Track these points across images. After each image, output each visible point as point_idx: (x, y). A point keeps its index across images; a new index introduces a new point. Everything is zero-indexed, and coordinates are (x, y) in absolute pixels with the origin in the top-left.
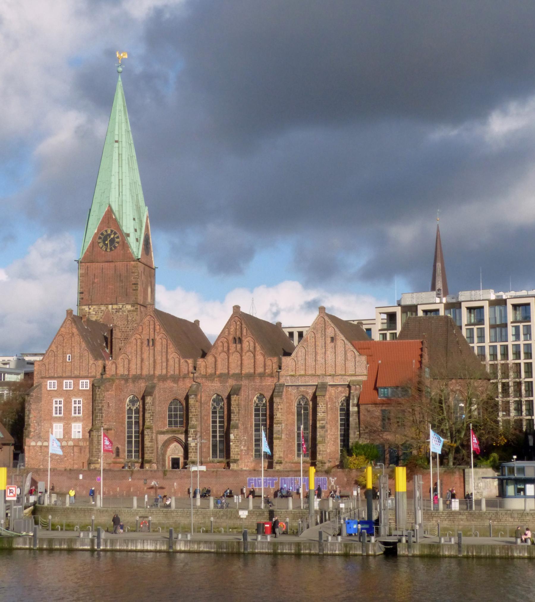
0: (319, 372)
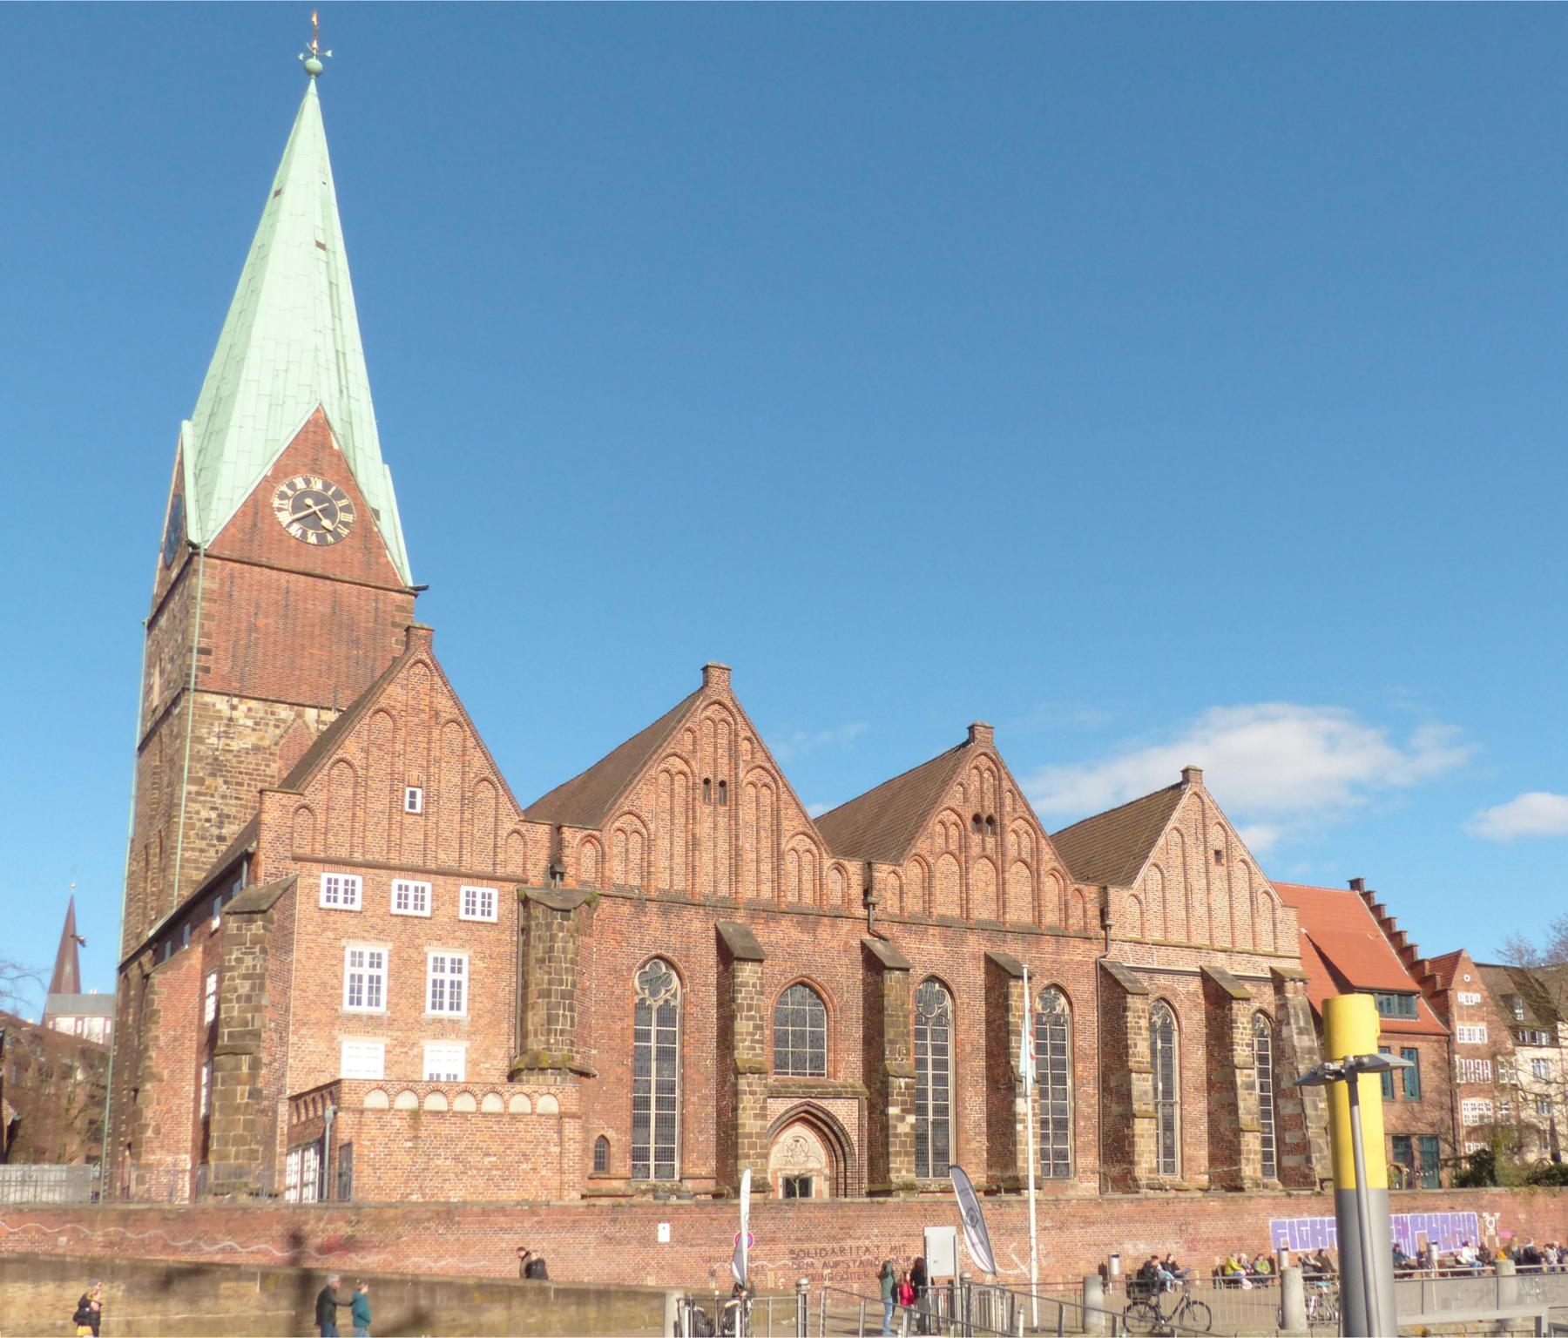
0: (1200, 939)
